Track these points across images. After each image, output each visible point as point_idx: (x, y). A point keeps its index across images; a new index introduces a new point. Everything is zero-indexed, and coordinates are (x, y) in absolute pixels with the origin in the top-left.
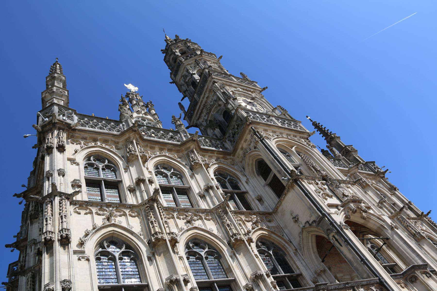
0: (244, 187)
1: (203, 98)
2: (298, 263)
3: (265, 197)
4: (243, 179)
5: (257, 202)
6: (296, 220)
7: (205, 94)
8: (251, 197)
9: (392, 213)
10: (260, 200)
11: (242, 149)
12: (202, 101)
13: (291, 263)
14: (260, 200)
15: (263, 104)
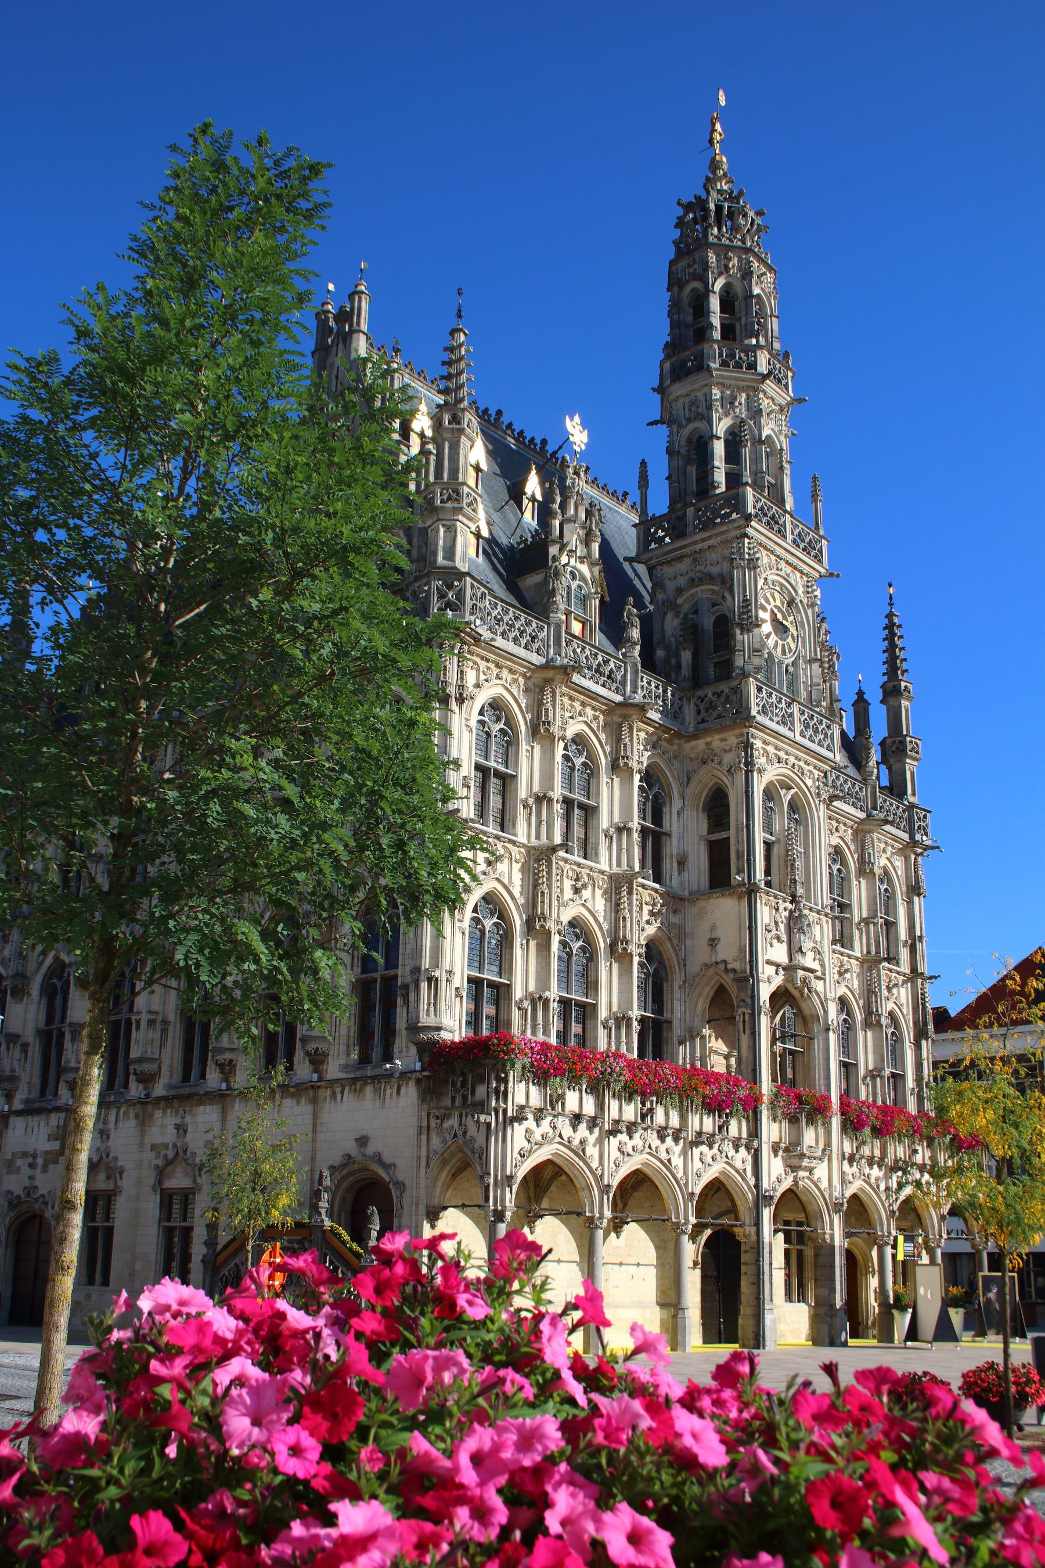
0: (671, 822)
1: (703, 540)
2: (677, 1004)
3: (691, 864)
4: (677, 804)
5: (675, 865)
6: (713, 942)
7: (710, 537)
8: (672, 848)
9: (868, 952)
10: (682, 863)
11: (708, 744)
12: (695, 543)
13: (666, 997)
14: (682, 863)
15: (803, 627)
